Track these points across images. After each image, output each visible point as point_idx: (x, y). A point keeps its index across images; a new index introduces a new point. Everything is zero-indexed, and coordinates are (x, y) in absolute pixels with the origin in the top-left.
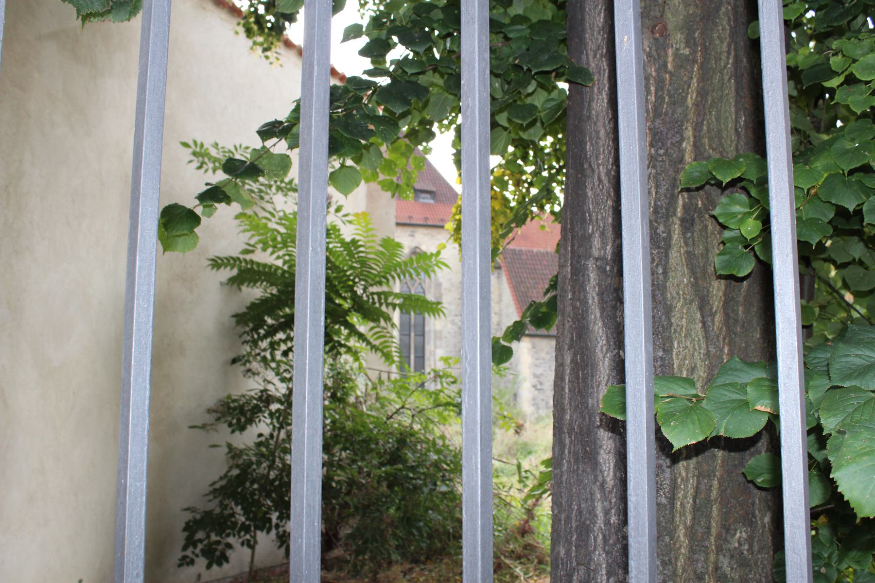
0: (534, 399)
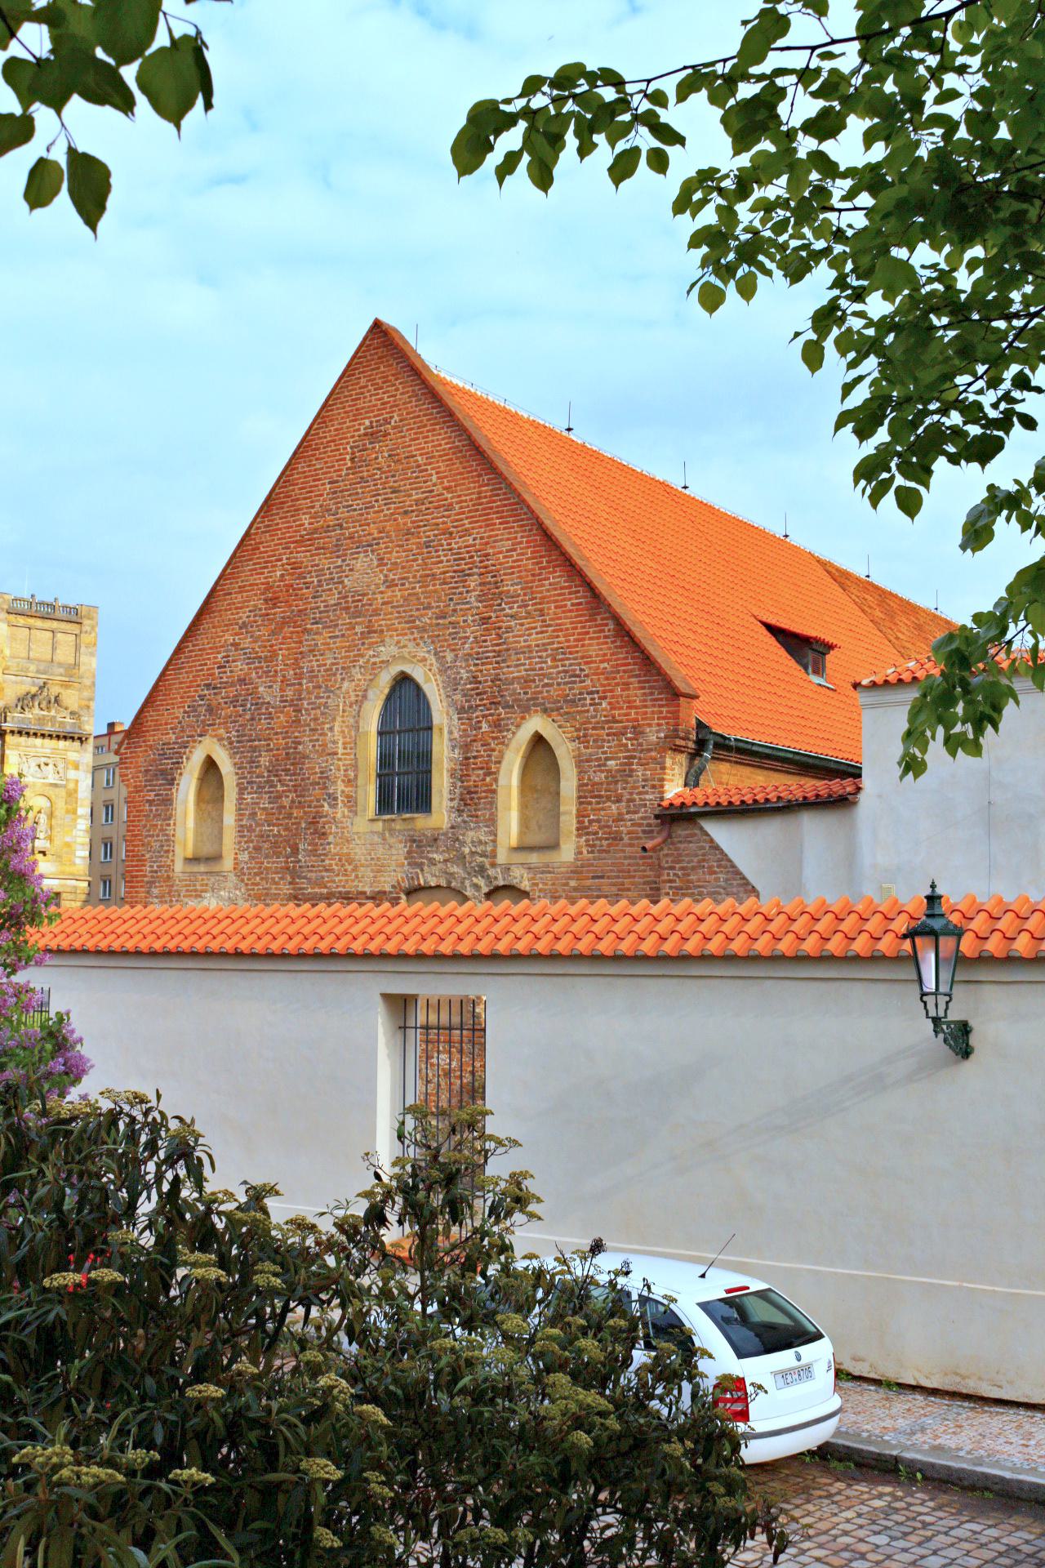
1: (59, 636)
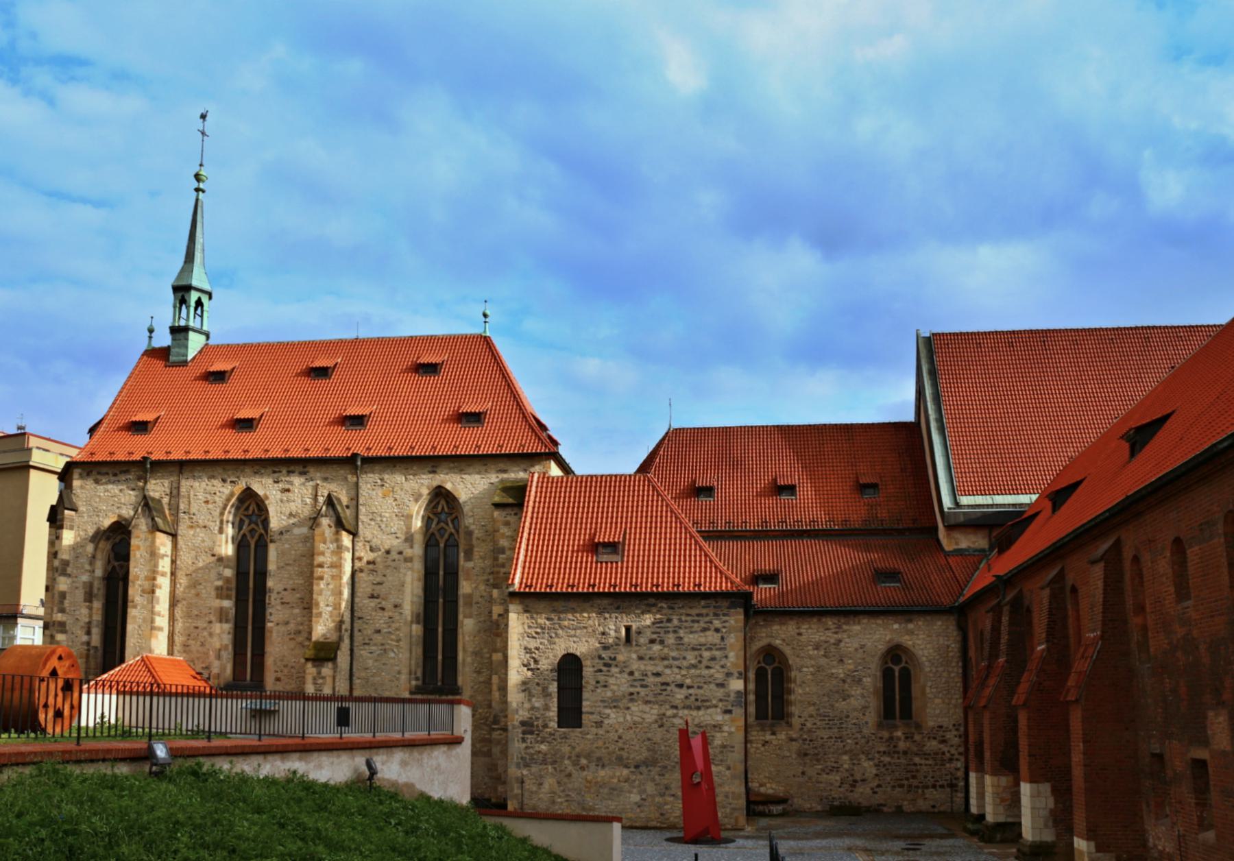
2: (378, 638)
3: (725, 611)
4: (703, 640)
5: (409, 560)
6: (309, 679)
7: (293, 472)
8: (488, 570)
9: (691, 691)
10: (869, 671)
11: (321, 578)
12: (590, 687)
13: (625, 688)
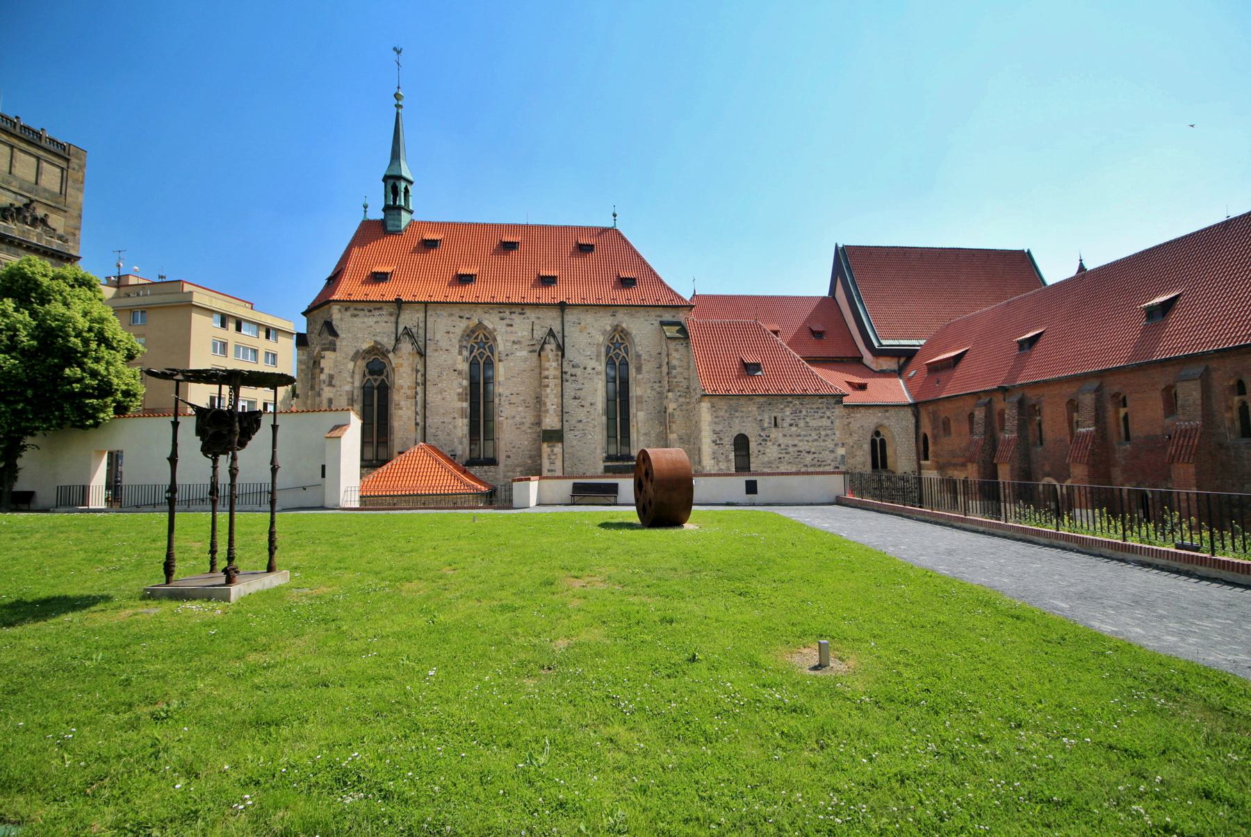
0: (714, 453)
1: (45, 165)
2: (580, 426)
3: (833, 406)
4: (820, 424)
5: (598, 374)
6: (545, 456)
7: (514, 313)
8: (653, 380)
9: (815, 455)
10: (866, 441)
11: (548, 386)
12: (755, 455)
13: (776, 455)
